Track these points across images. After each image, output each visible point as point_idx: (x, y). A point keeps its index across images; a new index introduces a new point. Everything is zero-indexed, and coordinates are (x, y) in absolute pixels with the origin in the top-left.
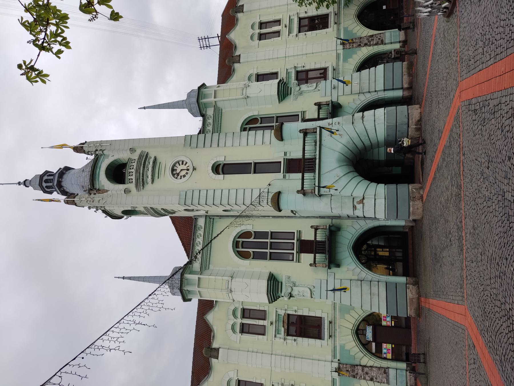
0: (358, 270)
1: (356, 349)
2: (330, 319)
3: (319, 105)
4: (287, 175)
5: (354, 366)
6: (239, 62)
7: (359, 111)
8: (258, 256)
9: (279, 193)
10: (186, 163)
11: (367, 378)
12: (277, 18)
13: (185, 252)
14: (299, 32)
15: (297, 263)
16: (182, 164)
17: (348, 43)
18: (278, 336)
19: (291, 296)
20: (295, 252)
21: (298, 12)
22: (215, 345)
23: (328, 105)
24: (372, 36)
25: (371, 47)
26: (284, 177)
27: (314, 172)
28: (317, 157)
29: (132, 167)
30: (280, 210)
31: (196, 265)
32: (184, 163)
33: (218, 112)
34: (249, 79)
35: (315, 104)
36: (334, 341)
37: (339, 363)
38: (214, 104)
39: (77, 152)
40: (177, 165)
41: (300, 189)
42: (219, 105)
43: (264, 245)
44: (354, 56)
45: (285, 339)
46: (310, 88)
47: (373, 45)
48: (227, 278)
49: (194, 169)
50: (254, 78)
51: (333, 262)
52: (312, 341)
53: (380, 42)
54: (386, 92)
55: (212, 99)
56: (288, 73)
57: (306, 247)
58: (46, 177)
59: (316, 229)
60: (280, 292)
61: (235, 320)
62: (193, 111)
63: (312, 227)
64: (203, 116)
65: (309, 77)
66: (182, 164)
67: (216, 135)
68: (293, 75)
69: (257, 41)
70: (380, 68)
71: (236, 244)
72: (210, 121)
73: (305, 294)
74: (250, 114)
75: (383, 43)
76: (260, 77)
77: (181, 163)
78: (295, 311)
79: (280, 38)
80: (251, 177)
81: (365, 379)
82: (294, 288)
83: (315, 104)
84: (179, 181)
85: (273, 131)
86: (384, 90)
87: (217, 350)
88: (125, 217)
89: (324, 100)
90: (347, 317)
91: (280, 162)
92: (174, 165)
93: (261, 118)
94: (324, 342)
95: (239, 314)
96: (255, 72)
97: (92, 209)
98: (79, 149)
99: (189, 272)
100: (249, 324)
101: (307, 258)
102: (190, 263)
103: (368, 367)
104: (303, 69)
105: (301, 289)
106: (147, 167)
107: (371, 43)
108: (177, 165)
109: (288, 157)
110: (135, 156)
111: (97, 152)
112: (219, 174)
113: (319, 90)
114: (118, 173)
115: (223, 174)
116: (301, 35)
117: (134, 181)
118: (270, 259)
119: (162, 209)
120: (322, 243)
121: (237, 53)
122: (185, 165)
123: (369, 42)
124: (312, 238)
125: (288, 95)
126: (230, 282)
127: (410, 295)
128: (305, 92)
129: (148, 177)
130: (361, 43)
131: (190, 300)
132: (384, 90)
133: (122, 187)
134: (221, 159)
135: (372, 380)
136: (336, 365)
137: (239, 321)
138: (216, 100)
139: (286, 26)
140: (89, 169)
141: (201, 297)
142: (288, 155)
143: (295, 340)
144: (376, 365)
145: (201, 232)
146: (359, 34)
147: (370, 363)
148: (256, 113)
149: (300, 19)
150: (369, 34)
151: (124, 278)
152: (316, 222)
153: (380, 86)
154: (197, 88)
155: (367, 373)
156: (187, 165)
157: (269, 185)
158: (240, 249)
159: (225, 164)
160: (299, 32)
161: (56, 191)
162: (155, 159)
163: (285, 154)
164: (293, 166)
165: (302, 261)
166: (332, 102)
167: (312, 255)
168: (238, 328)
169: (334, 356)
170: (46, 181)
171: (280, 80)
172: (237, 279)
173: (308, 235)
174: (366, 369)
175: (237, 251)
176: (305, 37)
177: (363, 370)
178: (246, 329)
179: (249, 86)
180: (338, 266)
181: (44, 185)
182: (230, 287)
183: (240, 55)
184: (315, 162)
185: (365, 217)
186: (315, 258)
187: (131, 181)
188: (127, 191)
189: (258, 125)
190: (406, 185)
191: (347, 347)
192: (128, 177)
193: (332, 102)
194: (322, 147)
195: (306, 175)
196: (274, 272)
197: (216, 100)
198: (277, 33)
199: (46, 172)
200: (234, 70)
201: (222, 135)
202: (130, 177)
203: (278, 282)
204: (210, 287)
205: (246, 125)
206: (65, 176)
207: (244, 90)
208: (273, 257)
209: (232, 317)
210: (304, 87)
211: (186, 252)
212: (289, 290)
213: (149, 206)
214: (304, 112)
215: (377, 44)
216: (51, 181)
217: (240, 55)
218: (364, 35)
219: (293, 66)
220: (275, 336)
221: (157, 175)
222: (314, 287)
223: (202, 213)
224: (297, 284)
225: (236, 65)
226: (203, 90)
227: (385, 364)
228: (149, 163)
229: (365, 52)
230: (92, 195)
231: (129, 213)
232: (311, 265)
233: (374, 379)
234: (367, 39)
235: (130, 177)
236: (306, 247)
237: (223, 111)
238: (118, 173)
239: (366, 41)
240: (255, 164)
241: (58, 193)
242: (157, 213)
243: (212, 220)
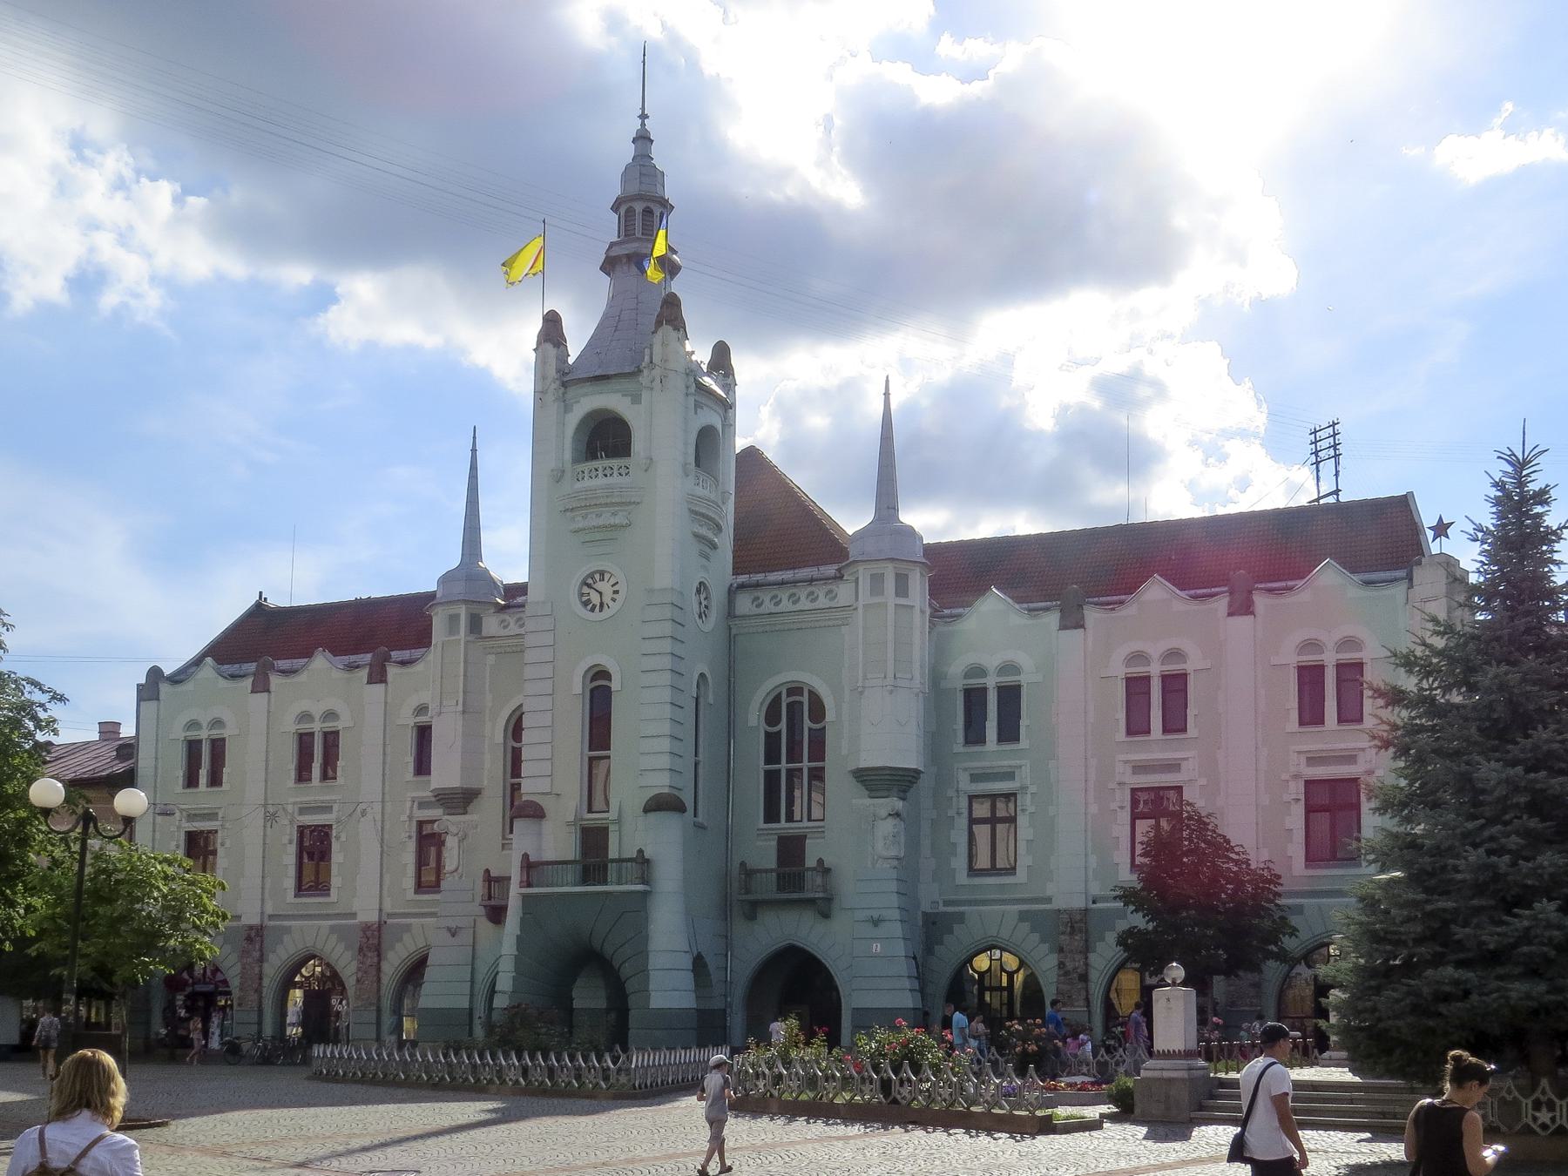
26: (568, 824)
46: (880, 845)
85: (666, 790)
109: (611, 828)
111: (646, 372)
148: (830, 716)
163: (615, 822)
164: (593, 839)
172: (460, 723)
181: (622, 210)
184: (600, 883)
189: (807, 723)
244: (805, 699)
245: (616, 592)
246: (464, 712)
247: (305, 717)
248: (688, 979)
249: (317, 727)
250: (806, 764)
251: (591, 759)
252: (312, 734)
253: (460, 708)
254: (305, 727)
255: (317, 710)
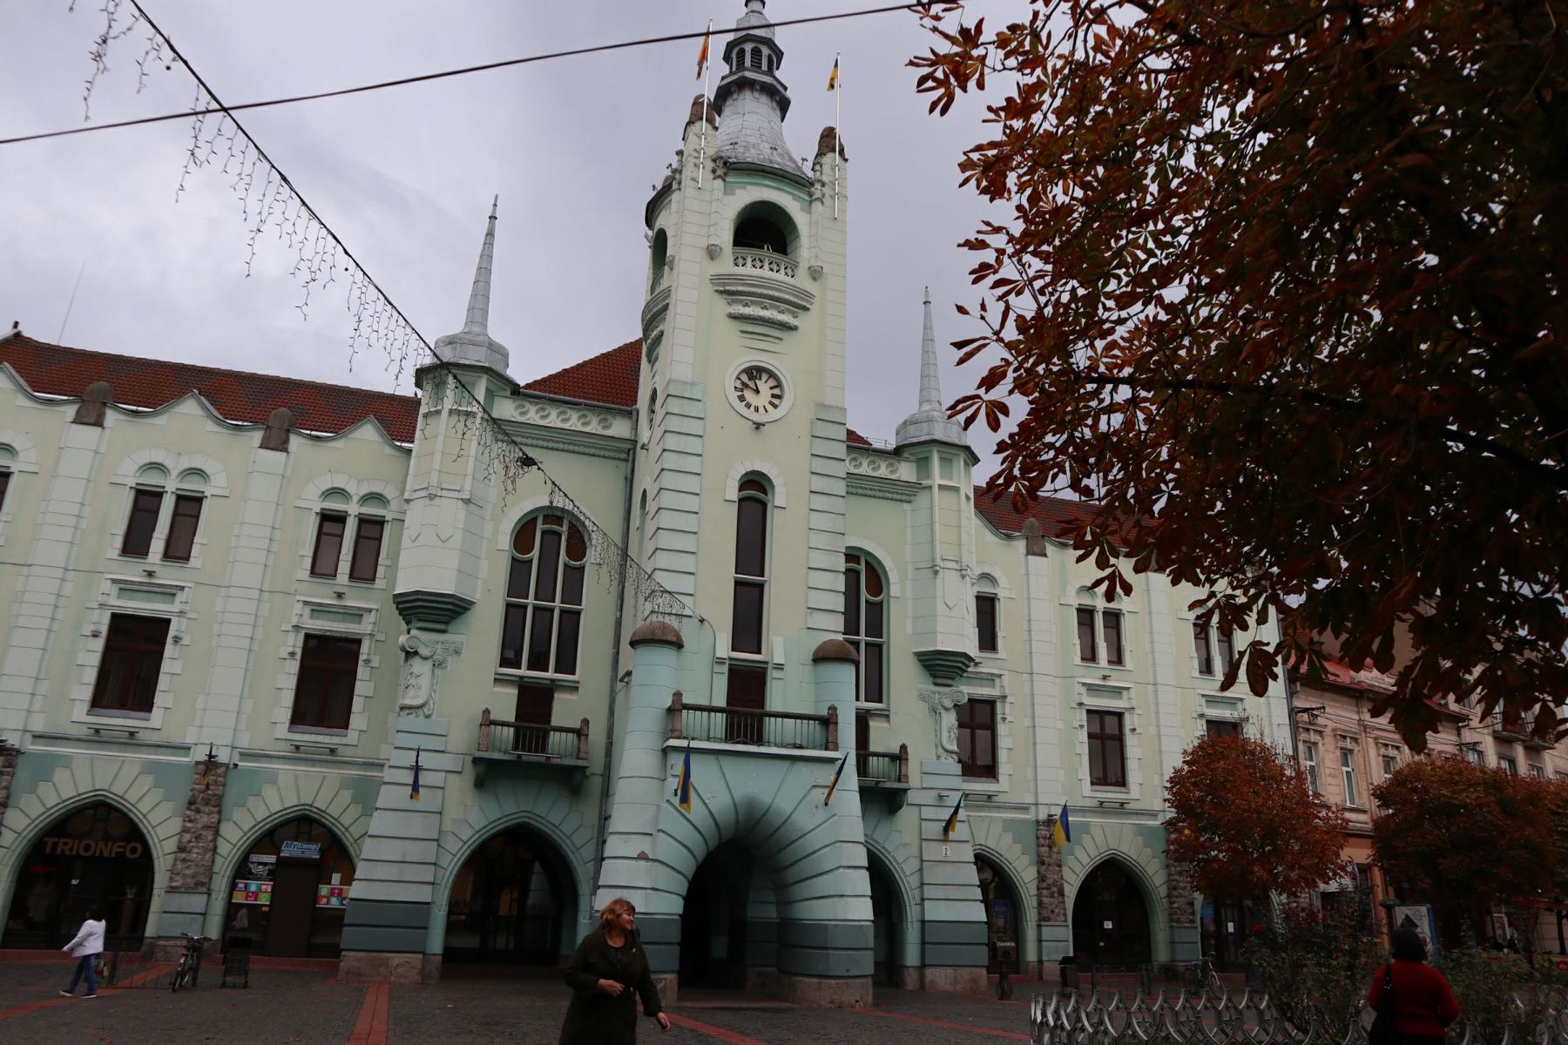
0: (466, 833)
1: (261, 814)
2: (341, 750)
3: (900, 757)
4: (725, 669)
5: (218, 803)
6: (1029, 552)
7: (872, 857)
8: (518, 570)
9: (678, 645)
10: (775, 406)
11: (187, 837)
12: (1127, 656)
13: (545, 375)
14: (1089, 711)
15: (493, 676)
16: (773, 396)
17: (1052, 833)
18: (307, 609)
19: (410, 654)
20: (523, 671)
21: (1137, 711)
22: (295, 442)
23: (899, 780)
24: (1061, 893)
25: (1034, 891)
26: (720, 661)
27: (726, 741)
28: (763, 750)
29: (775, 267)
30: (633, 644)
31: (506, 409)
32: (776, 401)
33: (906, 493)
34: (986, 577)
35: (903, 748)
36: (284, 758)
37: (227, 766)
38: (925, 483)
39: (822, 137)
40: (772, 383)
41: (685, 700)
42: (922, 499)
43: (545, 591)
44: (1017, 848)
45: (297, 628)
46: (945, 735)
47: (1039, 896)
48: (468, 487)
49: (758, 426)
50: (987, 589)
51: (489, 773)
52: (288, 698)
53: (1045, 913)
54: (917, 926)
55: (937, 479)
56: (991, 679)
57: (535, 704)
58: (765, 51)
59: (580, 733)
60: (421, 624)
61: (355, 499)
62: (912, 429)
63: (586, 722)
64: (898, 452)
65: (978, 732)
66: (773, 396)
67: (841, 488)
68: (984, 691)
69: (1075, 601)
70: (978, 913)
71: (553, 515)
72: (883, 471)
73: (411, 692)
74: (893, 576)
75: (1043, 919)
76: (986, 607)
77: (776, 391)
78: (367, 661)
79: (1078, 660)
80: (728, 574)
81: (185, 830)
82: (429, 663)
83: (903, 748)
84: (730, 383)
85: (840, 637)
86: (923, 922)
87: (282, 447)
88: (650, 233)
89: (913, 768)
90: (346, 796)
91: (759, 652)
92: (772, 375)
93: (881, 603)
94: (282, 730)
95: (371, 510)
96: (1002, 592)
97: (676, 158)
98: (828, 140)
99: (492, 387)
100: (341, 536)
101: (505, 704)
102: (516, 391)
103: (214, 840)
104: (999, 717)
105: (425, 681)
106: (772, 307)
107: (1045, 892)
108: (772, 383)
109: (772, 674)
110: (802, 280)
111: (818, 186)
112: (741, 489)
113: (938, 757)
114: (763, 231)
115: (741, 500)
116: (1082, 716)
117: (740, 270)
118: (509, 606)
119: (662, 334)
120: (542, 745)
121: (1050, 549)
122: (771, 403)
123: (1049, 884)
124: (555, 722)
125: (934, 676)
126: (456, 495)
127: (396, 959)
128: (938, 722)
129: (746, 305)
130: (1048, 863)
131: (418, 384)
132: (923, 922)
133: (726, 236)
134: (779, 497)
135: (181, 849)
136: (223, 757)
137: (353, 509)
138: (936, 489)
139: (1105, 678)
140: (778, 161)
141: (426, 416)
142: (776, 674)
143: (292, 654)
144: (219, 861)
145: (594, 426)
146: (1070, 861)
147: (224, 848)
148: (894, 590)
149: (1119, 716)
150: (1067, 888)
151: (493, 218)
152: (597, 733)
153: (935, 912)
154: (969, 443)
155: (198, 837)
156: (769, 407)
157: (702, 621)
158: (540, 526)
159: (764, 505)
160: (1089, 711)
161: (731, 73)
162: (793, 328)
163: (779, 667)
164: (747, 686)
165: (499, 689)
166: (905, 790)
167: (511, 718)
168: (335, 505)
169: (245, 756)
170: (756, 53)
171: (970, 659)
172: (462, 514)
173: (565, 710)
174: (209, 835)
175: (535, 519)
176: (1077, 724)
177: (207, 827)
178: (328, 527)
179: (963, 577)
180: (480, 784)
181: (748, 47)
182: (444, 493)
183: (1045, 555)
184: (752, 743)
185: (603, 859)
186: (503, 724)
187: (740, 261)
188: (712, 253)
189: (864, 594)
190: (676, 966)
191: (269, 792)
192: (750, 253)
193: (905, 790)
194: (787, 764)
195: (720, 719)
196: (474, 616)
197: (936, 489)
198: (1090, 656)
199: (779, 55)
200: (1009, 537)
201: (838, 505)
202: (749, 260)
203: (447, 623)
204: (449, 442)
205: (867, 563)
206: (764, 99)
207: (953, 565)
208: (513, 614)
209: (364, 490)
210: (950, 719)
211: (544, 380)
212: (424, 651)
213: (672, 301)
214: (887, 716)
215: (1040, 903)
216: (756, 65)
217: (1045, 555)
218: (1066, 873)
219: (1007, 692)
220: (306, 603)
221: (750, 328)
222: (427, 717)
223: (644, 435)
224: (438, 672)
225: (1020, 545)
226: (962, 456)
227: (220, 884)
228: (782, 312)
229: (1025, 874)
230: (710, 165)
231: (659, 244)
232: (487, 712)
233: (183, 855)
234: (1055, 883)
235: (749, 260)
236: (535, 704)
237: (906, 506)
238: (763, 231)
239: (1051, 878)
240: (761, 586)
241: (723, 78)
242: (654, 316)
243: (624, 456)
244: (863, 567)
245: (757, 409)
246: (467, 501)
247: (157, 467)
248: (861, 882)
249: (171, 485)
250: (862, 637)
251: (737, 583)
252: (158, 495)
253: (466, 496)
254: (152, 480)
255: (176, 465)
